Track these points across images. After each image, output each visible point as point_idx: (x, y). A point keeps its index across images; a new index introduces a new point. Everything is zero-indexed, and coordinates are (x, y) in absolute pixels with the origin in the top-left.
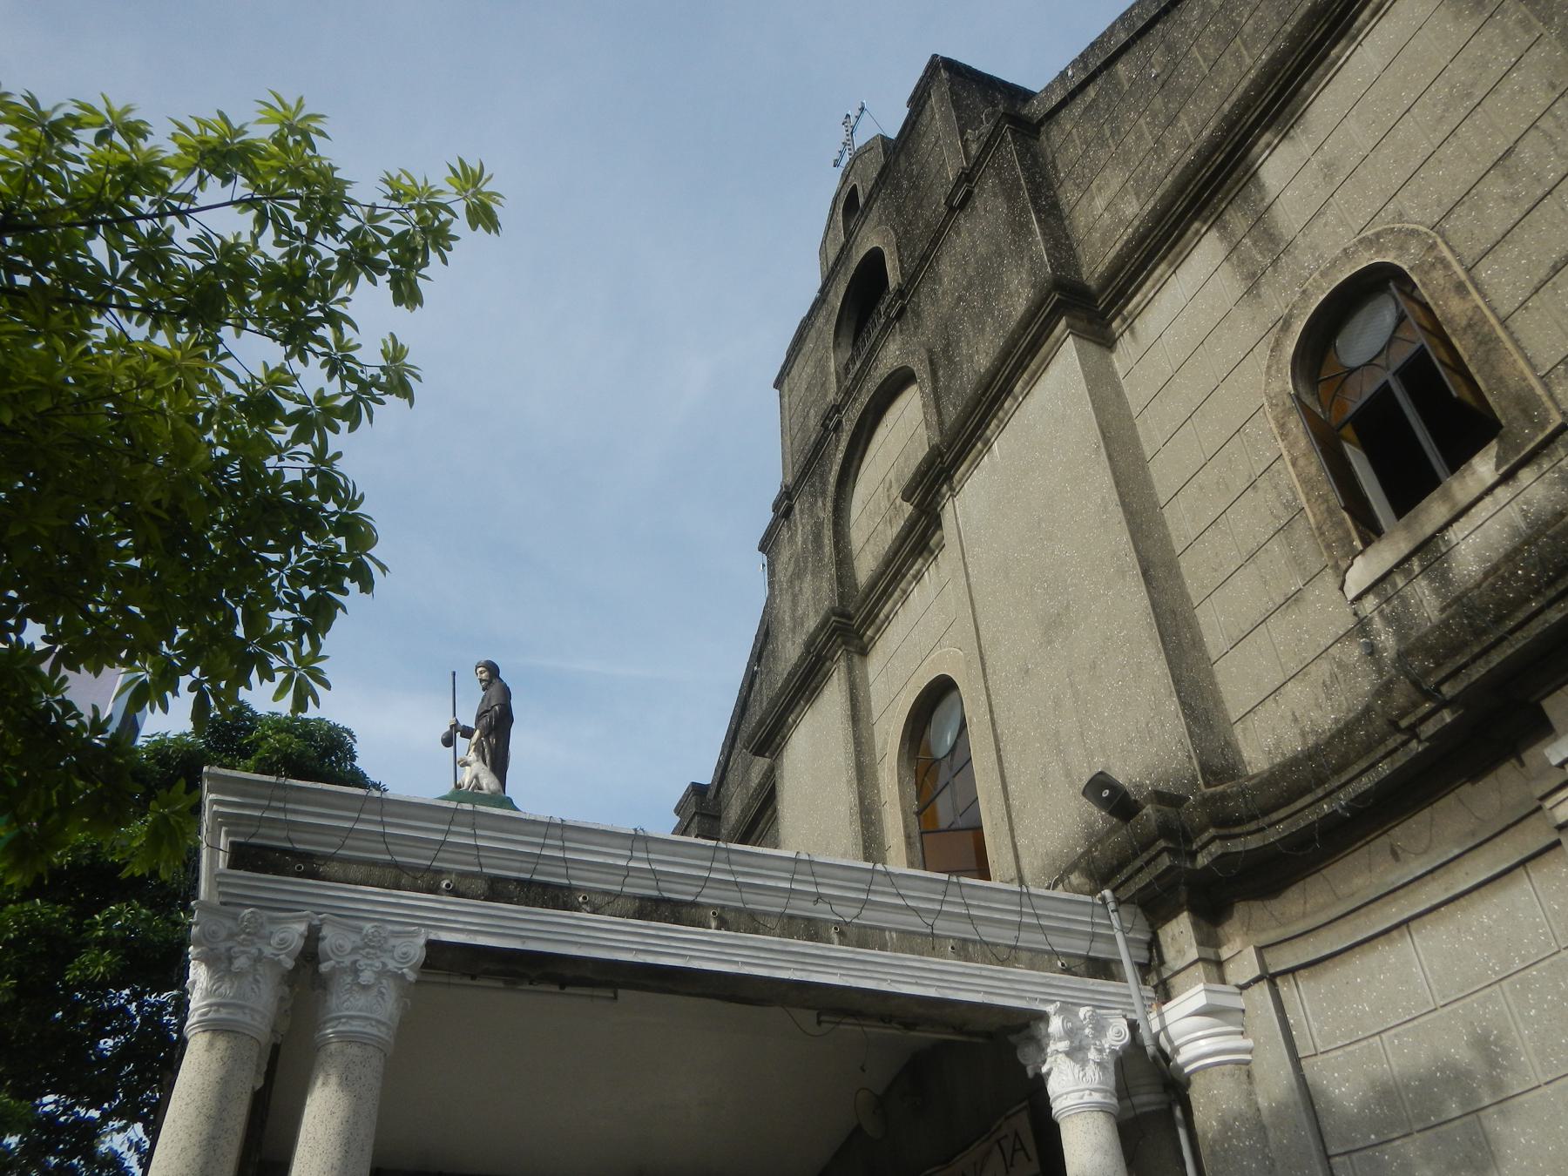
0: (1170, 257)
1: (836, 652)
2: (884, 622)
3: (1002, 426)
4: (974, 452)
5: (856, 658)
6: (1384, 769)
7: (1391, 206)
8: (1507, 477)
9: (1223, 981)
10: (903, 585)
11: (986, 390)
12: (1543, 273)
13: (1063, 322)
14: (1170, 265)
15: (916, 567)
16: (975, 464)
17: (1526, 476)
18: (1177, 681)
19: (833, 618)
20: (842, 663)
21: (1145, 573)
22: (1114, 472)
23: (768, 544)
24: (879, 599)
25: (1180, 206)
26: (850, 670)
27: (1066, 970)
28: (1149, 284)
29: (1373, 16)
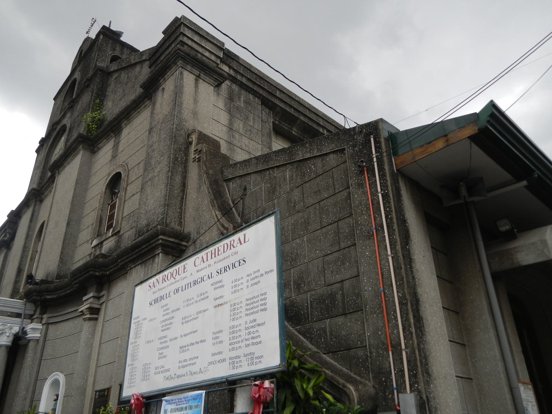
3: (69, 163)
5: (38, 203)
6: (72, 290)
9: (41, 323)
13: (81, 146)
17: (114, 237)
18: (62, 253)
19: (33, 191)
20: (33, 204)
21: (68, 224)
22: (74, 194)
23: (38, 151)
24: (45, 190)
26: (35, 206)
27: (9, 316)
29: (145, 107)
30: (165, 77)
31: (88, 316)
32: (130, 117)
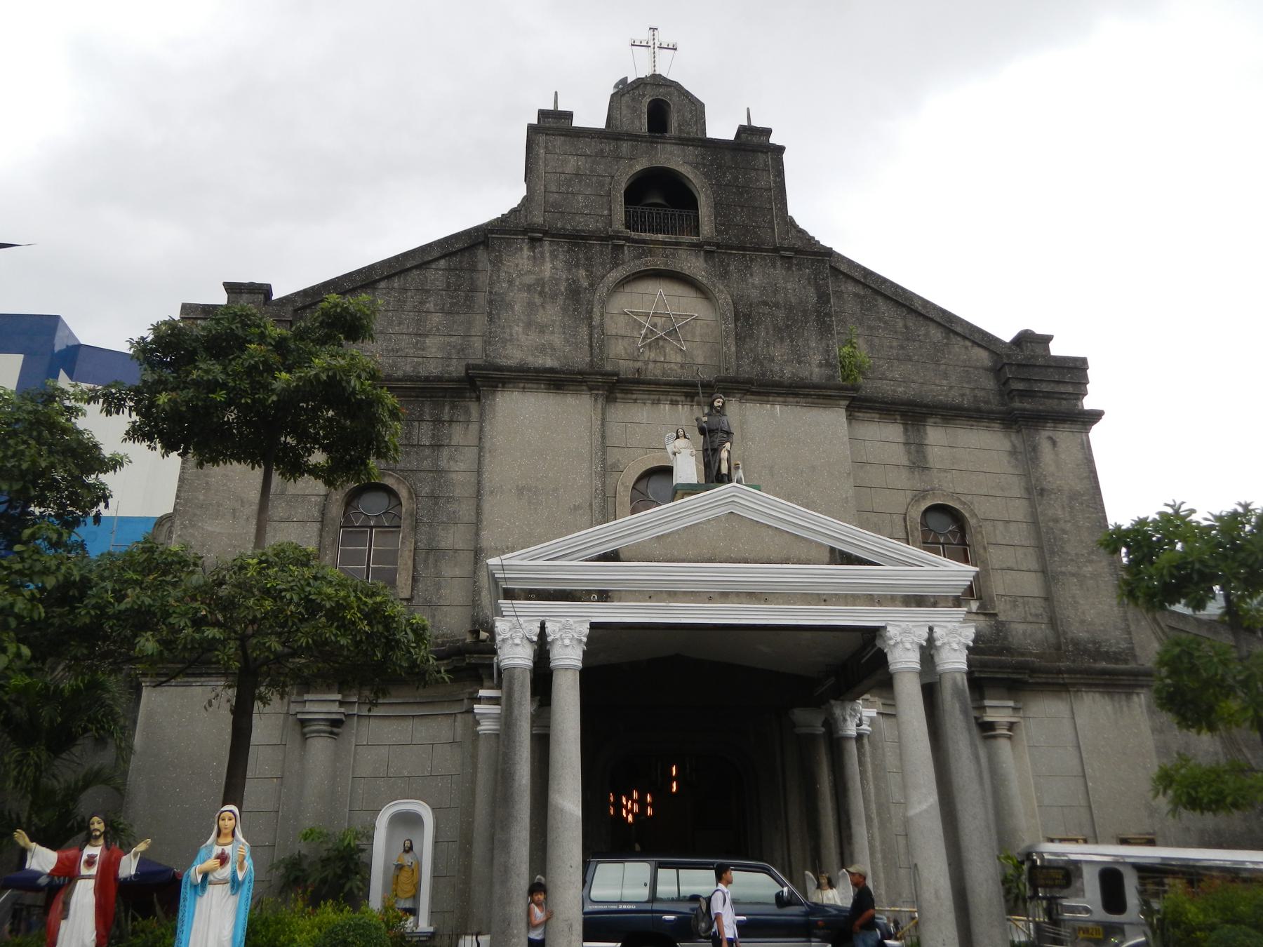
0: (883, 416)
1: (598, 390)
2: (630, 399)
3: (785, 403)
4: (765, 398)
7: (970, 497)
8: (977, 613)
10: (661, 397)
11: (797, 388)
12: (1004, 566)
14: (879, 418)
15: (679, 399)
16: (761, 402)
17: (982, 618)
25: (903, 408)
28: (868, 415)
30: (1058, 425)
31: (1006, 732)
32: (952, 422)
